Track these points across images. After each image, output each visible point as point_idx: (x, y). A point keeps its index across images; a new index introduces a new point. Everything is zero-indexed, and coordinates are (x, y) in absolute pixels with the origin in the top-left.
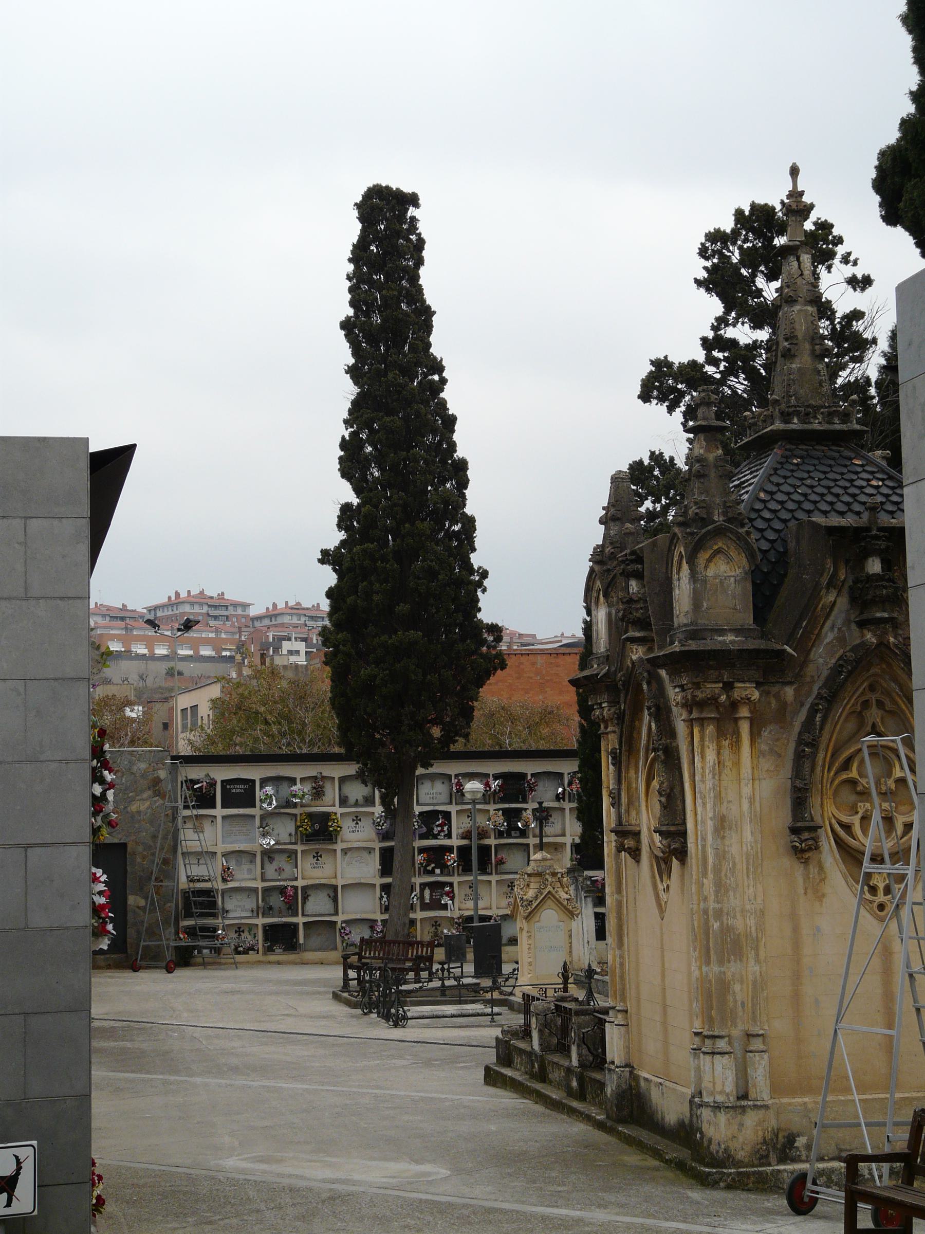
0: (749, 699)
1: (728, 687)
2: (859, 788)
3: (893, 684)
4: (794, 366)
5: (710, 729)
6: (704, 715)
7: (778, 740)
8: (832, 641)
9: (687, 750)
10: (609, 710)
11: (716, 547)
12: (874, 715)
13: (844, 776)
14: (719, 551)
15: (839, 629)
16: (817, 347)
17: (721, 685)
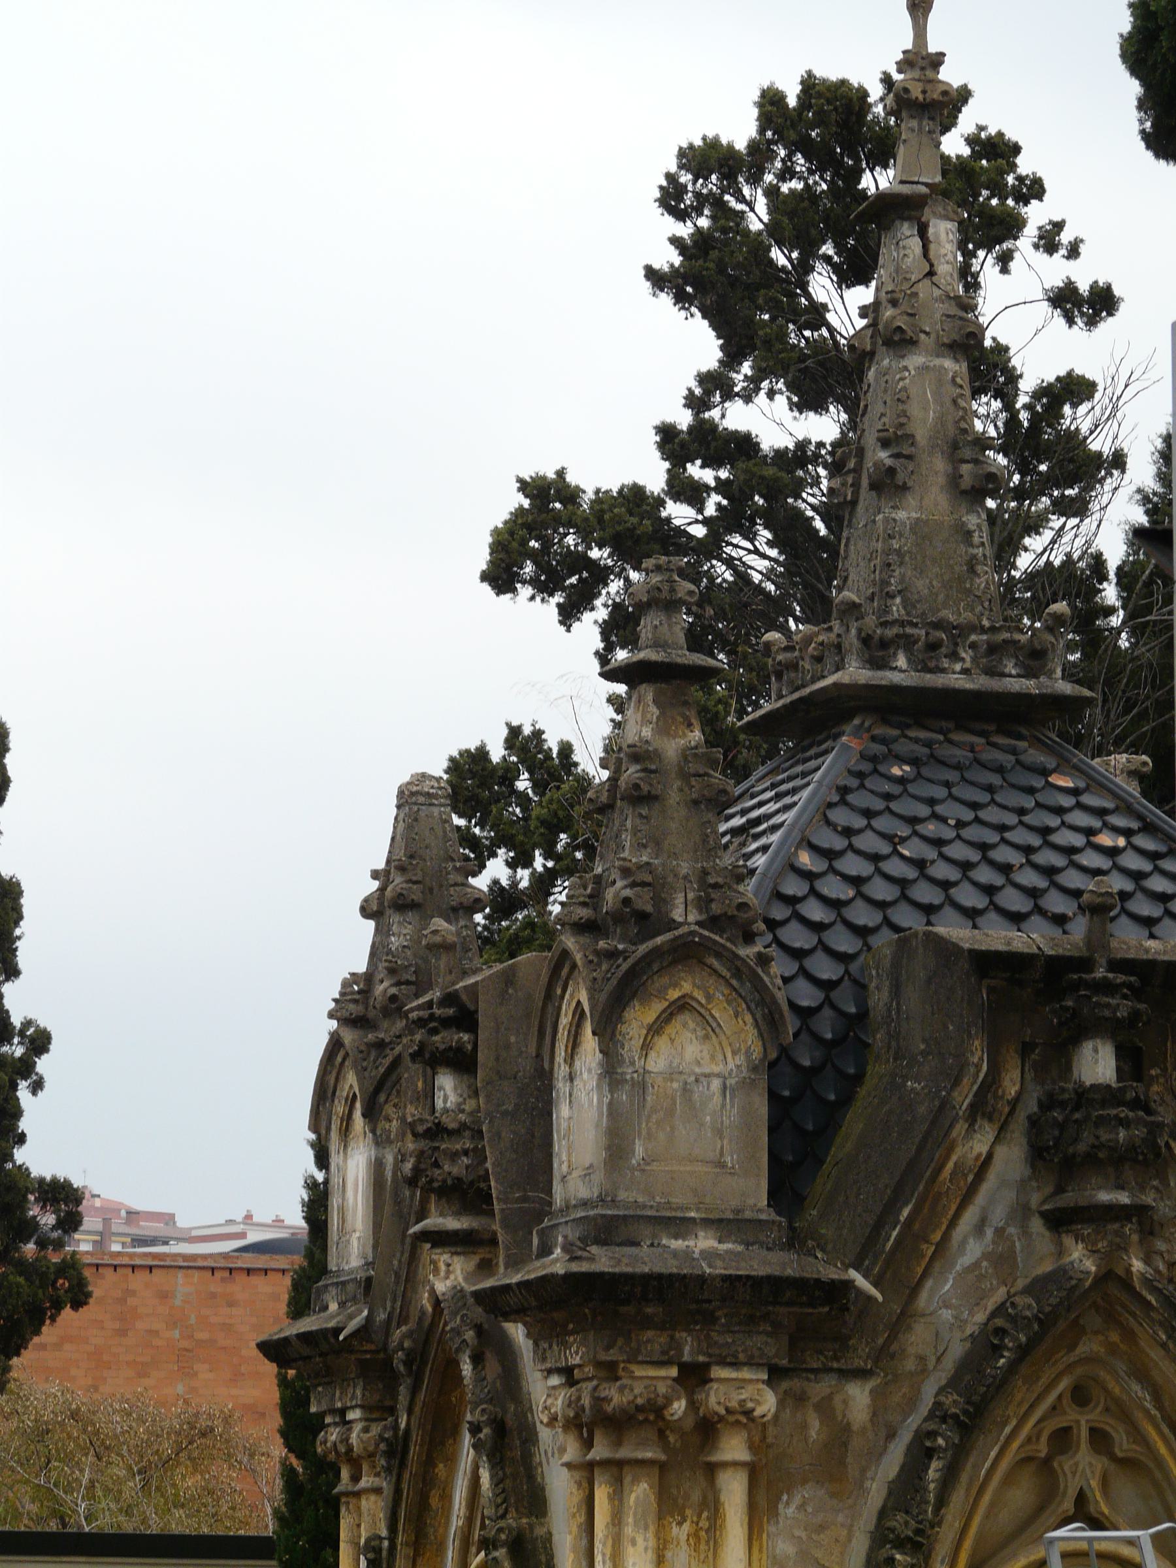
0: (748, 1413)
1: (694, 1377)
3: (1136, 1387)
4: (901, 515)
5: (640, 1492)
6: (624, 1453)
7: (822, 1528)
8: (976, 1265)
9: (574, 1550)
10: (366, 1430)
11: (674, 994)
12: (1083, 1468)
14: (682, 1006)
15: (999, 1232)
16: (965, 468)
17: (674, 1372)
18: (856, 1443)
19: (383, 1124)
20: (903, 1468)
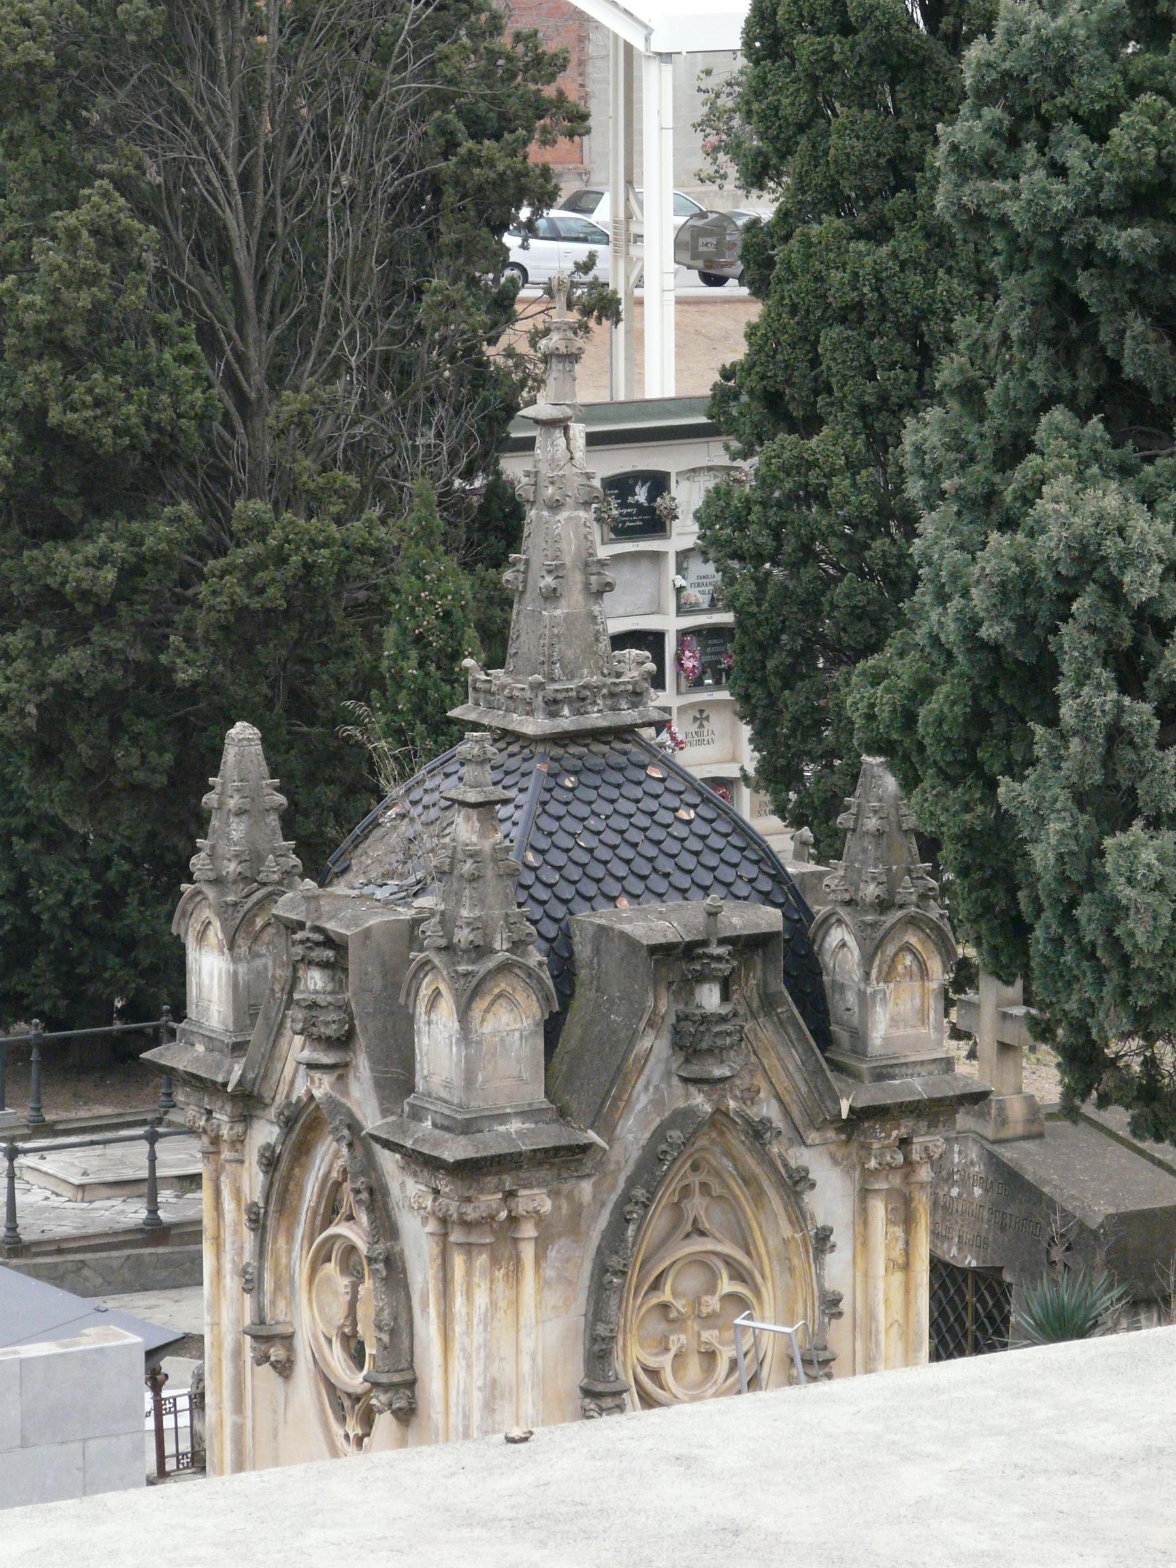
0: (537, 1212)
1: (510, 1195)
2: (673, 1315)
4: (558, 612)
5: (482, 1260)
6: (473, 1239)
7: (568, 1260)
8: (645, 1108)
9: (435, 1278)
10: (231, 1128)
11: (497, 991)
12: (697, 1205)
13: (654, 1300)
14: (500, 996)
15: (657, 1087)
16: (593, 579)
17: (500, 1195)
18: (585, 1213)
19: (237, 950)
20: (610, 1223)
